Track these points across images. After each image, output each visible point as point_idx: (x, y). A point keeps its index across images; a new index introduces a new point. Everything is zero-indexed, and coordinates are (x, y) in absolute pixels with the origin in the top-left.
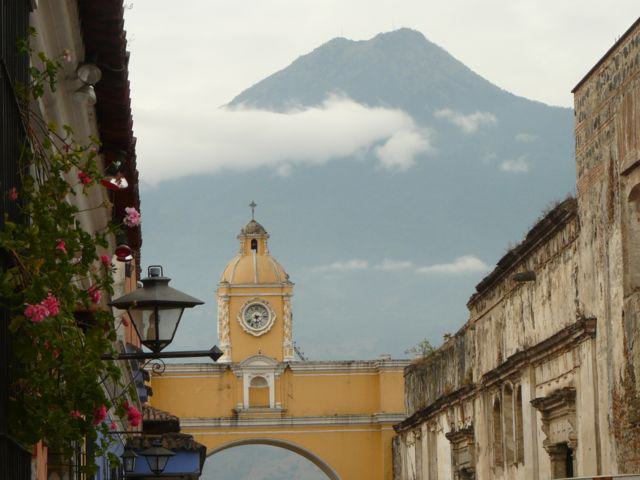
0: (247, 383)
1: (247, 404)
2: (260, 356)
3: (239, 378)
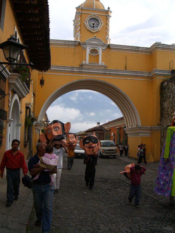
0: (88, 51)
1: (87, 62)
3: (85, 49)
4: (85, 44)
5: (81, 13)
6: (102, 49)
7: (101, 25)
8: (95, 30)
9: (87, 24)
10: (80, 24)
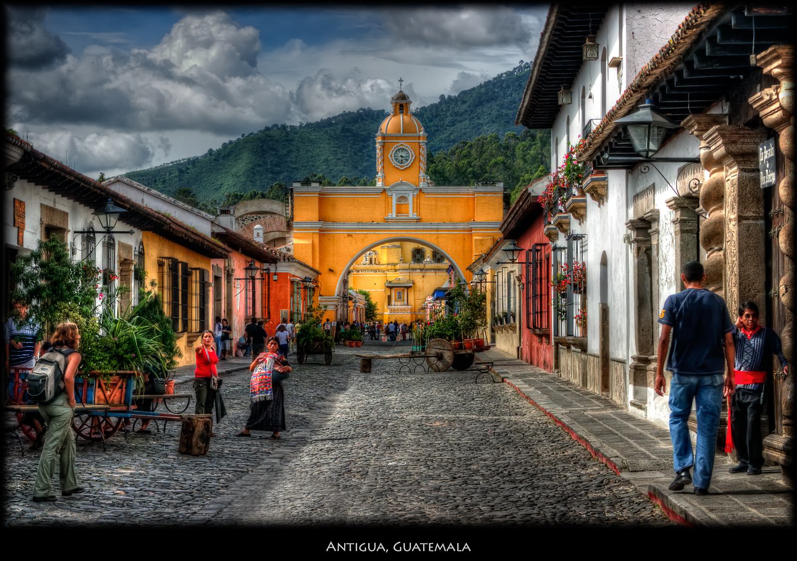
5: (384, 143)
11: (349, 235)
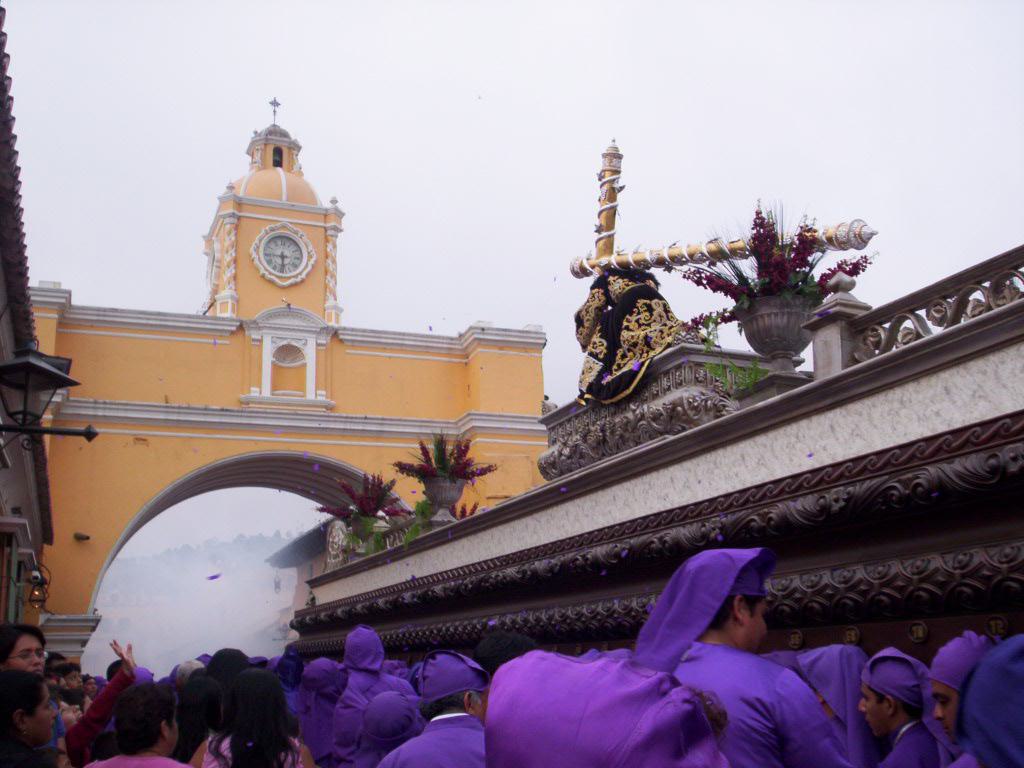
2: (289, 310)
4: (255, 325)
5: (239, 218)
6: (318, 345)
7: (308, 260)
8: (289, 278)
9: (258, 254)
10: (234, 255)
11: (139, 440)
